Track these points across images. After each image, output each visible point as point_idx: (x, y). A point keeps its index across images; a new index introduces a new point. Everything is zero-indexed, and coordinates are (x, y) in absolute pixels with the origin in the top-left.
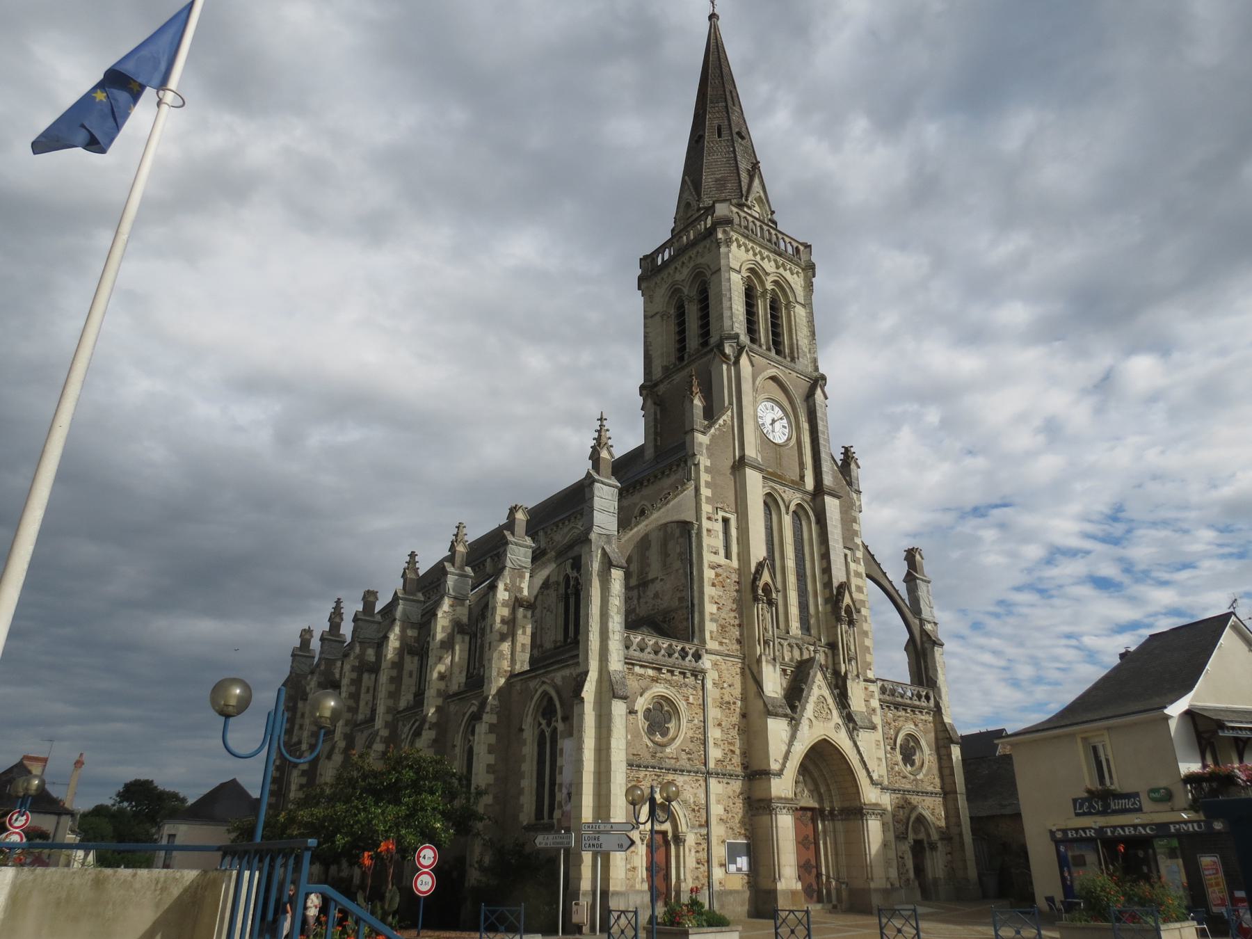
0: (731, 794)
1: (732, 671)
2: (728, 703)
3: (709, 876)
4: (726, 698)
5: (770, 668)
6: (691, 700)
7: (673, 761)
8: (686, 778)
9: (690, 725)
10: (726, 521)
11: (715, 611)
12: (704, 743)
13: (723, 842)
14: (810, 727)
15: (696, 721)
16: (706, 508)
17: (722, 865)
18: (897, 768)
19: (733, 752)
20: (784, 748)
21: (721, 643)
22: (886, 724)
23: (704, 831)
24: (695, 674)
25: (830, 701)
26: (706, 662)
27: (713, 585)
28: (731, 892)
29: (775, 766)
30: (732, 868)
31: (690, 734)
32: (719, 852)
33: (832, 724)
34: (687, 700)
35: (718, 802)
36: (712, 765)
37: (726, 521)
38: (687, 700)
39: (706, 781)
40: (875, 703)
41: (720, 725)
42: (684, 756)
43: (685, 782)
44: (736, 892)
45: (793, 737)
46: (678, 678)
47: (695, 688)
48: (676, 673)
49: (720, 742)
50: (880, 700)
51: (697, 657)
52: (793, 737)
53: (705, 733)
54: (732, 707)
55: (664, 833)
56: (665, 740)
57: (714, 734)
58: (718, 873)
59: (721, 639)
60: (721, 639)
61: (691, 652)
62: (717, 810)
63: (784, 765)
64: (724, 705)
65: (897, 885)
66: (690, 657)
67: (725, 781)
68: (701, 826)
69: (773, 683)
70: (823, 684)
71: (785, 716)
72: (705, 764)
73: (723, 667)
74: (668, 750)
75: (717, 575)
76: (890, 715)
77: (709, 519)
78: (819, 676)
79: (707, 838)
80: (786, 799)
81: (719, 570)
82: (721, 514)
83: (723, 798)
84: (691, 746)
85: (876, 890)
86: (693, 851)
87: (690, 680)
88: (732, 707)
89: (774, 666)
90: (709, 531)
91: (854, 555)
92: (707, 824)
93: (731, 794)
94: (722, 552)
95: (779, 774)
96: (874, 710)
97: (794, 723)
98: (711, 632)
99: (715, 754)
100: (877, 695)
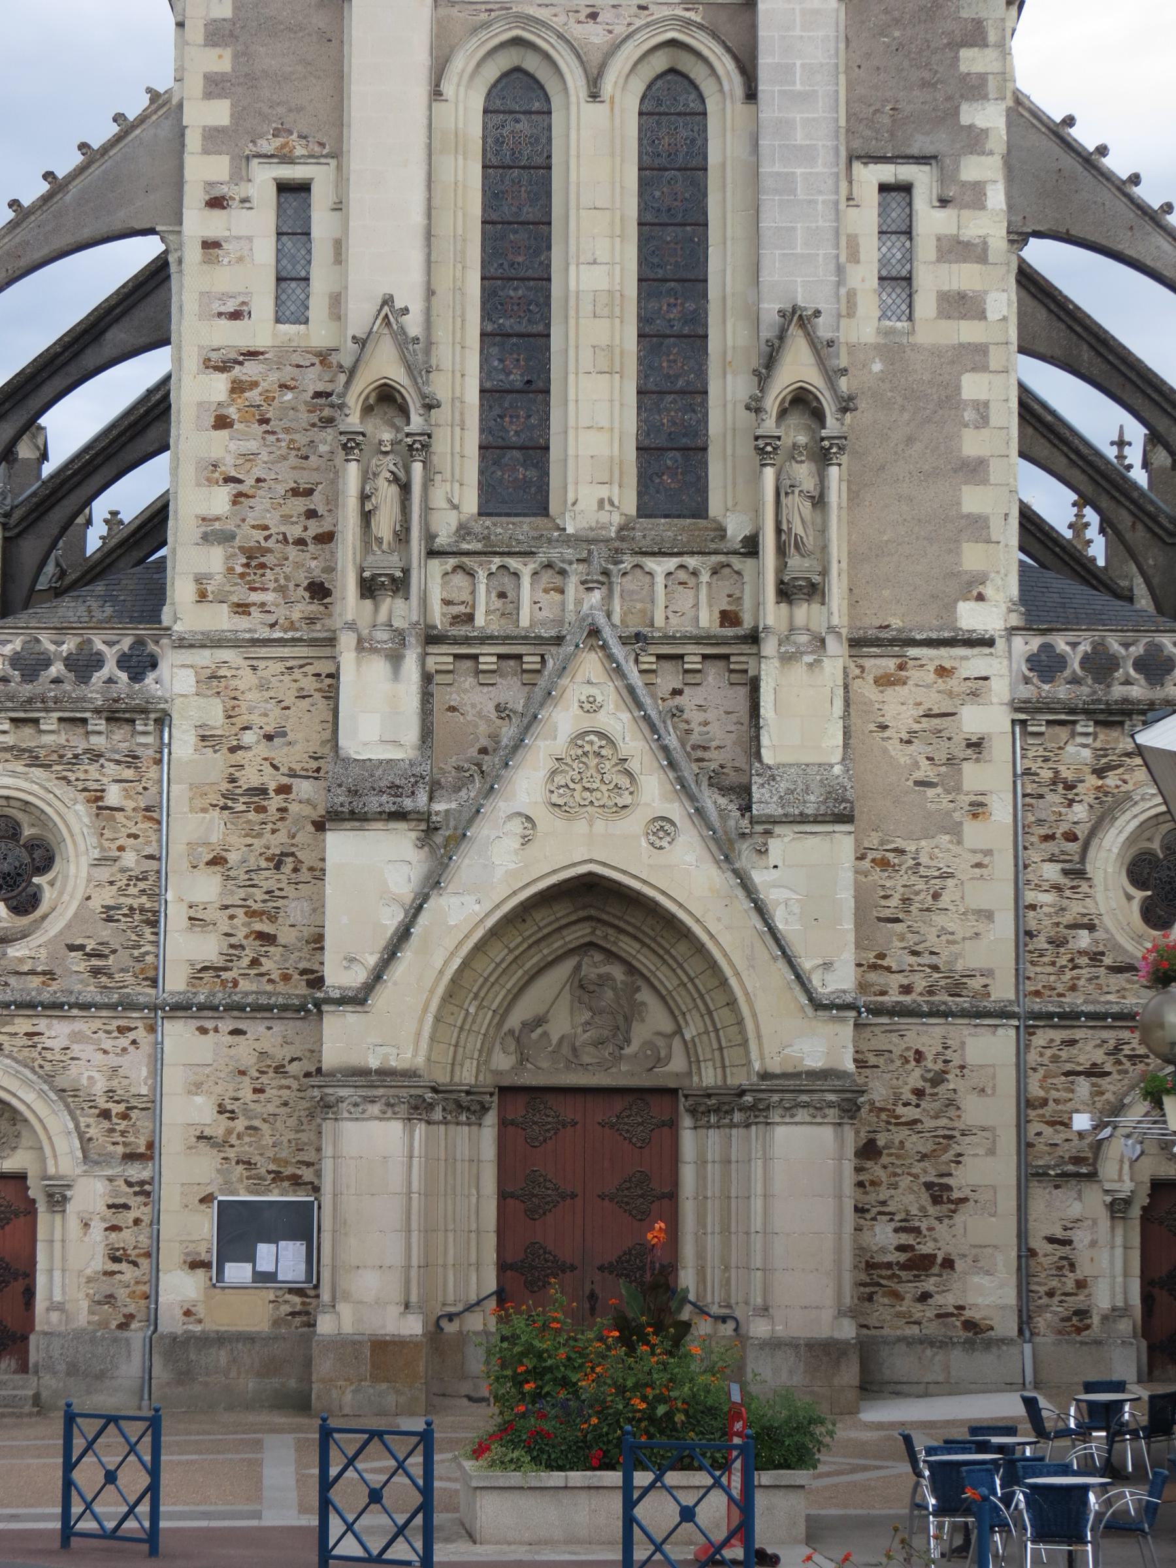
0: (248, 1060)
1: (266, 688)
2: (262, 791)
3: (151, 1297)
4: (250, 778)
5: (378, 667)
6: (114, 795)
7: (36, 981)
8: (79, 1026)
9: (104, 874)
10: (293, 192)
11: (219, 500)
12: (154, 924)
13: (206, 1199)
14: (526, 841)
15: (129, 859)
16: (203, 169)
17: (195, 1265)
18: (1084, 940)
19: (267, 939)
20: (392, 919)
21: (242, 609)
22: (1028, 791)
23: (137, 1172)
24: (117, 715)
25: (634, 744)
26: (175, 678)
27: (222, 423)
28: (221, 1339)
29: (340, 976)
30: (238, 1272)
31: (107, 896)
32: (190, 1227)
33: (634, 824)
34: (96, 798)
35: (196, 1087)
36: (175, 982)
37: (293, 192)
38: (96, 798)
39: (152, 1029)
40: (989, 718)
41: (217, 861)
42: (78, 964)
43: (76, 1037)
44: (249, 1339)
45: (433, 883)
46: (52, 735)
47: (132, 760)
48: (50, 722)
49: (210, 915)
50: (1019, 706)
51: (139, 664)
52: (433, 883)
53: (155, 894)
54: (275, 802)
55: (20, 1178)
56: (25, 921)
57: (192, 889)
58: (180, 1288)
59: (241, 594)
60: (241, 594)
61: (111, 655)
62: (186, 1111)
63: (377, 977)
64: (242, 799)
65: (1007, 1326)
66: (110, 668)
67: (226, 1026)
68: (130, 1157)
69: (379, 714)
70: (608, 694)
71: (399, 815)
72: (154, 982)
73: (246, 680)
74: (15, 951)
75: (238, 388)
76: (1077, 753)
77: (217, 203)
78: (591, 665)
79: (145, 1190)
80: (385, 1074)
81: (251, 370)
82: (265, 177)
83: (191, 1075)
84: (106, 932)
85: (774, 1345)
86: (98, 1228)
87: (117, 740)
88: (275, 802)
89: (395, 659)
90: (211, 245)
91: (946, 177)
92: (149, 1154)
93: (248, 1060)
94: (263, 305)
95: (358, 999)
96: (976, 745)
97: (442, 842)
98: (199, 580)
99: (185, 951)
100: (1001, 689)
